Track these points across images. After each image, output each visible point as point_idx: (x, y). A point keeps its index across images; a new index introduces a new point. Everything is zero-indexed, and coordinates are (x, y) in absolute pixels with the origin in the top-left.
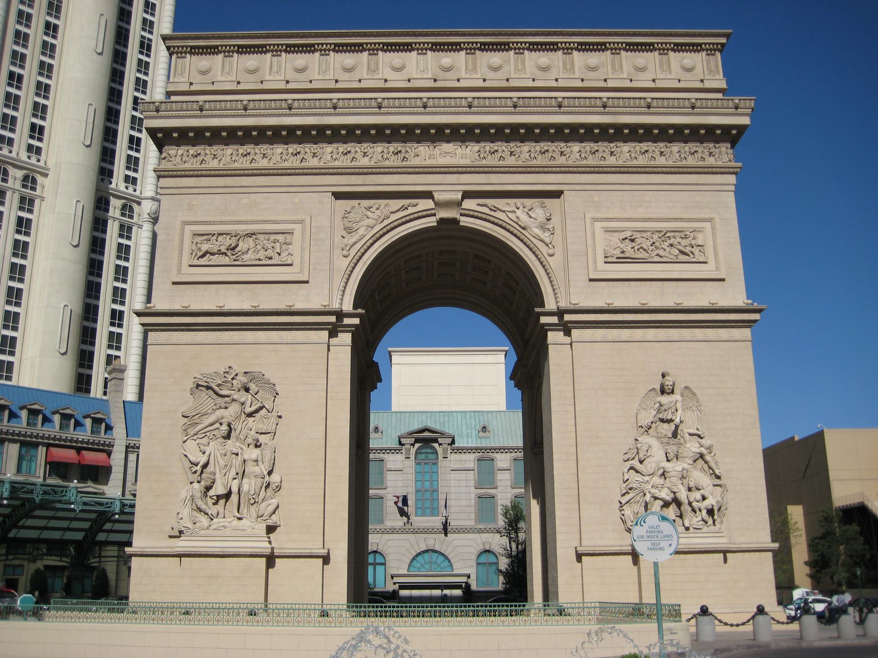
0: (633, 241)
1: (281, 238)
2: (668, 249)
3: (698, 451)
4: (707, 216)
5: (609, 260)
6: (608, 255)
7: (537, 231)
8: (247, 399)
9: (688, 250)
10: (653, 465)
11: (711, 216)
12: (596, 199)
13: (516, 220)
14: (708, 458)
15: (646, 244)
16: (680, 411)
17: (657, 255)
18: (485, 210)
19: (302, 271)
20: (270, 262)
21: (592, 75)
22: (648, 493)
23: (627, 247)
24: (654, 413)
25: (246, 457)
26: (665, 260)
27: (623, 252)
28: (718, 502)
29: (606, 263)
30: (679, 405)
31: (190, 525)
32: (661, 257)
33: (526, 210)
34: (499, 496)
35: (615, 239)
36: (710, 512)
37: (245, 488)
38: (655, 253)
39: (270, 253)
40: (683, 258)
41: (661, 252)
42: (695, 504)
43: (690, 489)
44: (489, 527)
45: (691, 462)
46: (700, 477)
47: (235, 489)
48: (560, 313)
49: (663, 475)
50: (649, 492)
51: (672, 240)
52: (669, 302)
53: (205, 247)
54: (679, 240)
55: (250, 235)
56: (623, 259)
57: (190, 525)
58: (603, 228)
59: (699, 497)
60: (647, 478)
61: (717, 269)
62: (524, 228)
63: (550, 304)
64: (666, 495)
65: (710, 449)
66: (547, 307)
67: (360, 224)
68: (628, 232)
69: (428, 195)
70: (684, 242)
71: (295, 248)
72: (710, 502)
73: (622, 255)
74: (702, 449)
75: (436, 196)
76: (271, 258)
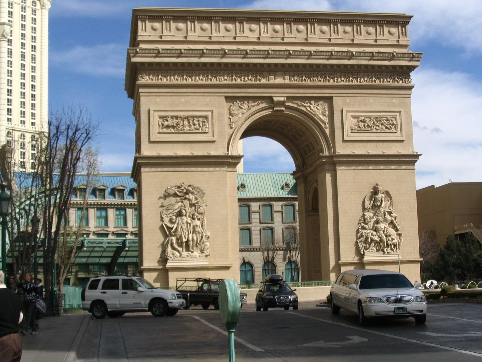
0: (364, 122)
1: (201, 119)
2: (380, 126)
3: (391, 219)
4: (398, 110)
5: (354, 131)
6: (353, 129)
7: (321, 117)
8: (192, 198)
9: (388, 126)
10: (372, 226)
11: (400, 110)
12: (348, 101)
13: (310, 111)
14: (395, 222)
15: (370, 124)
16: (384, 202)
17: (375, 129)
18: (295, 106)
19: (213, 136)
20: (197, 131)
21: (346, 36)
22: (369, 238)
23: (361, 125)
24: (372, 202)
25: (194, 224)
26: (379, 131)
27: (359, 127)
28: (398, 241)
29: (351, 132)
30: (383, 199)
31: (171, 256)
32: (377, 130)
33: (315, 106)
34: (253, 228)
35: (355, 121)
36: (395, 245)
37: (195, 238)
38: (374, 128)
39: (197, 126)
40: (386, 130)
41: (377, 128)
42: (390, 242)
43: (386, 236)
44: (247, 247)
45: (388, 224)
46: (391, 231)
47: (191, 239)
48: (331, 157)
49: (375, 230)
50: (370, 237)
51: (382, 121)
52: (380, 152)
53: (166, 123)
54: (385, 121)
55: (187, 118)
56: (360, 131)
57: (171, 256)
58: (351, 115)
59: (391, 239)
60: (369, 231)
61: (402, 135)
62: (315, 115)
63: (326, 153)
64: (376, 238)
65: (395, 218)
66: (325, 154)
67: (239, 112)
68: (362, 117)
69: (271, 98)
70: (387, 122)
71: (209, 125)
72: (396, 241)
73: (359, 129)
74: (392, 218)
75: (275, 99)
76: (198, 129)
